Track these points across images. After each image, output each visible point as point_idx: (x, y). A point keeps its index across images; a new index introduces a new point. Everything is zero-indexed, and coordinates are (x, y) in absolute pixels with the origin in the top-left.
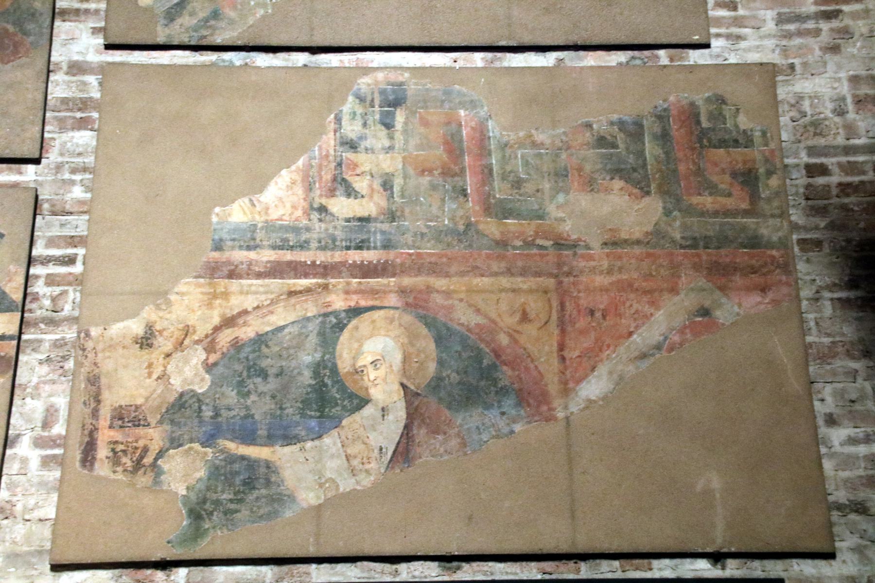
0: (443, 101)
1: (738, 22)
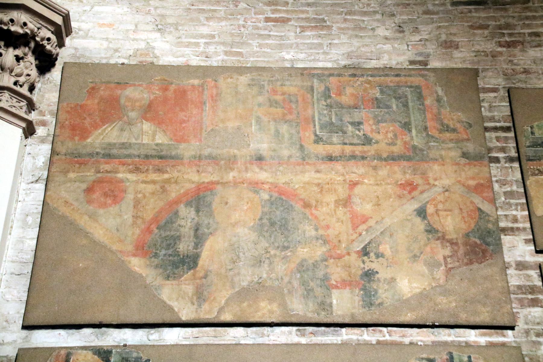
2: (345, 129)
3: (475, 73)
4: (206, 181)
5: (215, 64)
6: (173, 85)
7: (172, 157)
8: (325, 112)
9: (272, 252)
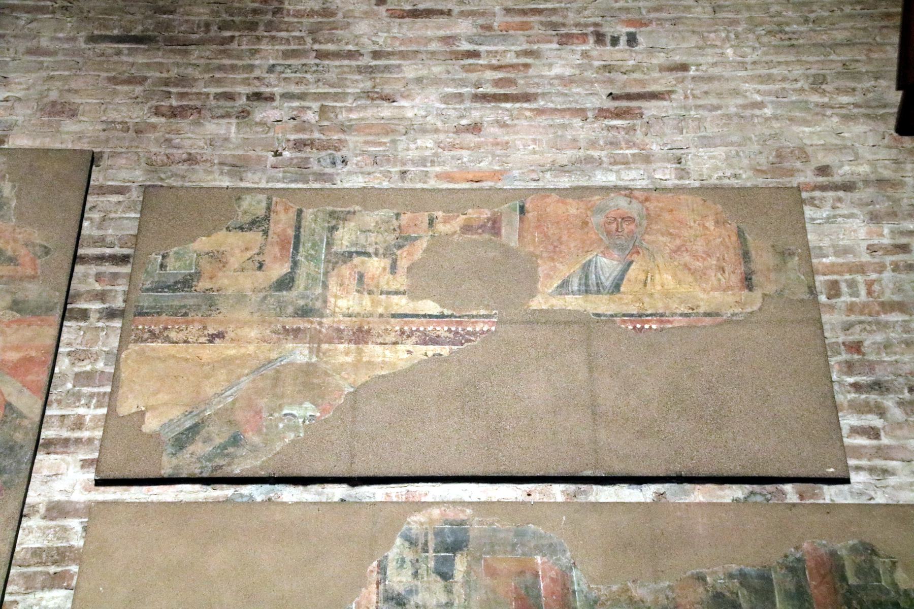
0: (514, 546)
1: (882, 452)
3: (94, 159)
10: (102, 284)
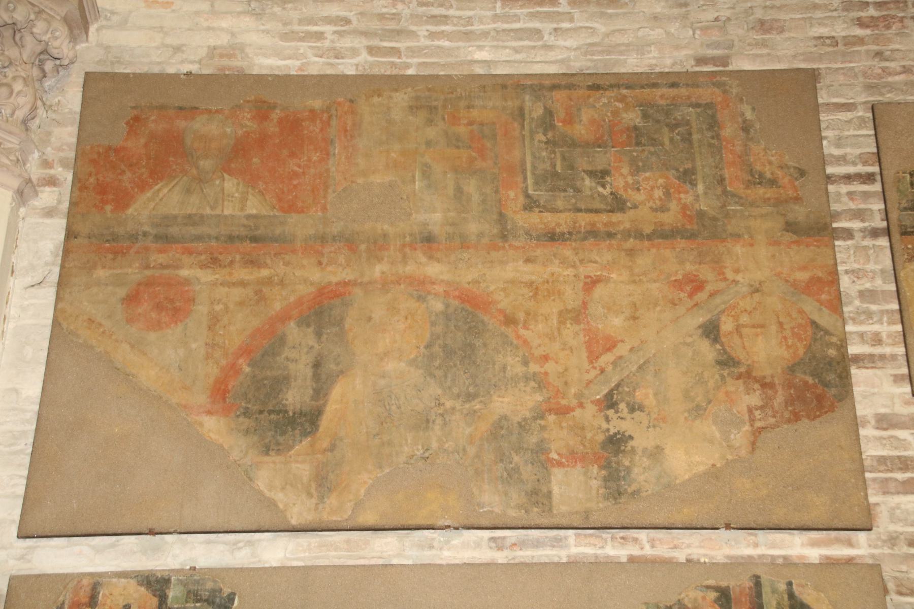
2: (578, 183)
4: (334, 279)
5: (351, 71)
6: (278, 111)
7: (275, 239)
8: (544, 154)
9: (448, 404)
10: (855, 202)
